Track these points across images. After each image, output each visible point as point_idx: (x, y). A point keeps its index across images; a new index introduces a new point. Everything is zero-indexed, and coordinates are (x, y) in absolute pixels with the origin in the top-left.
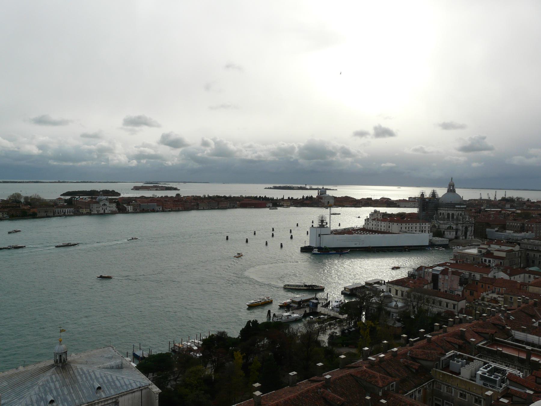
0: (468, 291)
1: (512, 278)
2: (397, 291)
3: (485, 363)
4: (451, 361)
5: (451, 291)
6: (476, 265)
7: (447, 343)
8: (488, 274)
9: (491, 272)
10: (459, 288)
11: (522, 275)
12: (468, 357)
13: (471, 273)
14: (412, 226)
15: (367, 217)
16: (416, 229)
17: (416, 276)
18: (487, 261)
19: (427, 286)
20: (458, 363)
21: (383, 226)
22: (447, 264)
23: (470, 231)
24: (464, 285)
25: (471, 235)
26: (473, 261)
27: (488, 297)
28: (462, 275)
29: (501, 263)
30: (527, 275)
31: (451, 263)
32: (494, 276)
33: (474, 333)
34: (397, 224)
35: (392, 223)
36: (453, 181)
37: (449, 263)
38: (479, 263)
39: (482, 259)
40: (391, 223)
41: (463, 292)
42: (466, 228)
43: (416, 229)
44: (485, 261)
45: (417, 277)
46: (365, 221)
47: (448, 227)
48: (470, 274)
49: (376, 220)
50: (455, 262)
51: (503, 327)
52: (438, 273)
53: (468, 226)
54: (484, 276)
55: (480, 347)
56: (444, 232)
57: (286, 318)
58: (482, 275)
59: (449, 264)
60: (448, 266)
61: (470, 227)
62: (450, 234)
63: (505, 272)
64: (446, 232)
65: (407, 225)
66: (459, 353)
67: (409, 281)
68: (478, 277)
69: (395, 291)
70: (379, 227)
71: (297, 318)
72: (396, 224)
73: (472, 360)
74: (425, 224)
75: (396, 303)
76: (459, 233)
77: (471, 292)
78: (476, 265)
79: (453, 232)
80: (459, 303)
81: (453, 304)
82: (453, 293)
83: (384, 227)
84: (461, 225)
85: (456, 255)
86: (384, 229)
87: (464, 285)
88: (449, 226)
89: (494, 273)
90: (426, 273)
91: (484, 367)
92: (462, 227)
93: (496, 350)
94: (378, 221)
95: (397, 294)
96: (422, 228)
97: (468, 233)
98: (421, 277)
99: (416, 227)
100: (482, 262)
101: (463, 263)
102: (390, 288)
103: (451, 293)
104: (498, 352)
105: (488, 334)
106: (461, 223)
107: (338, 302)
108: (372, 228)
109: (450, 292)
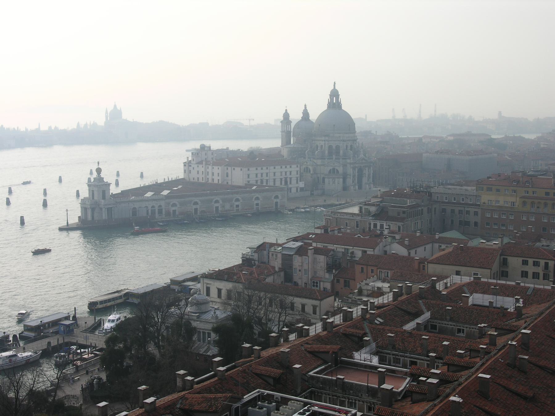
0: (342, 281)
1: (413, 252)
2: (219, 291)
3: (306, 404)
4: (250, 408)
5: (314, 282)
6: (359, 235)
7: (254, 375)
8: (374, 249)
9: (379, 244)
10: (327, 275)
11: (429, 247)
12: (282, 397)
13: (348, 249)
14: (268, 171)
15: (188, 158)
16: (274, 175)
17: (255, 260)
18: (378, 227)
19: (272, 277)
20: (261, 411)
21: (216, 174)
22: (310, 236)
23: (367, 176)
24: (334, 271)
25: (368, 183)
26: (356, 228)
27: (369, 288)
28: (332, 253)
29: (399, 227)
30: (436, 245)
31: (316, 234)
32: (384, 251)
33: (308, 355)
34: (241, 170)
35: (233, 168)
36: (336, 88)
37: (313, 234)
38: (364, 230)
39: (370, 224)
40: (229, 168)
41: (332, 283)
42: (361, 171)
43: (274, 175)
44: (375, 225)
45: (257, 263)
46: (185, 165)
47: (331, 169)
48: (346, 251)
49: (204, 163)
50: (323, 231)
51: (358, 337)
52: (292, 253)
53: (364, 166)
54: (368, 253)
55: (312, 377)
56: (324, 179)
57: (7, 360)
58: (365, 252)
59: (314, 236)
60: (311, 239)
61: (367, 168)
62: (334, 182)
63: (401, 243)
64: (326, 180)
65: (259, 171)
66: (267, 392)
67: (242, 271)
68: (358, 253)
69: (217, 290)
70: (210, 176)
71: (29, 359)
72: (239, 169)
73: (285, 401)
74: (291, 167)
75: (215, 313)
76: (349, 181)
77: (345, 281)
78: (359, 235)
79: (338, 178)
80: (322, 302)
81: (312, 305)
82: (317, 286)
83: (218, 176)
84: (352, 166)
85: (330, 219)
86: (218, 180)
87: (334, 271)
88: (331, 168)
89: (385, 247)
90: (273, 255)
91: (301, 411)
92: (354, 168)
93: (336, 378)
94: (207, 166)
95: (219, 296)
96: (286, 175)
97: (365, 180)
98: (264, 263)
99: (274, 173)
100: (370, 228)
101: (339, 232)
102: (208, 286)
103: (314, 286)
104: (338, 383)
105: (328, 352)
106: (352, 161)
107: (113, 321)
108: (198, 178)
109: (313, 284)
